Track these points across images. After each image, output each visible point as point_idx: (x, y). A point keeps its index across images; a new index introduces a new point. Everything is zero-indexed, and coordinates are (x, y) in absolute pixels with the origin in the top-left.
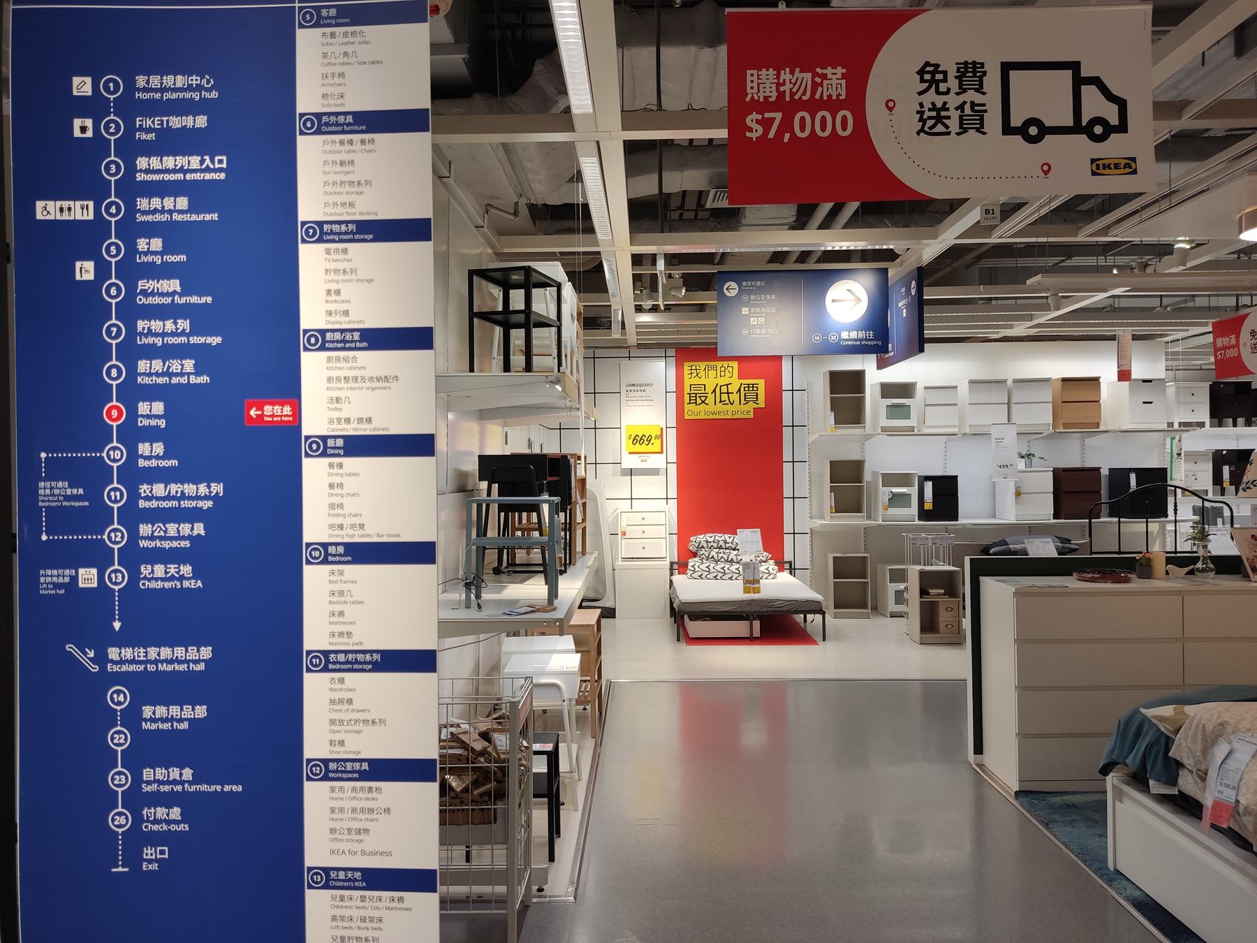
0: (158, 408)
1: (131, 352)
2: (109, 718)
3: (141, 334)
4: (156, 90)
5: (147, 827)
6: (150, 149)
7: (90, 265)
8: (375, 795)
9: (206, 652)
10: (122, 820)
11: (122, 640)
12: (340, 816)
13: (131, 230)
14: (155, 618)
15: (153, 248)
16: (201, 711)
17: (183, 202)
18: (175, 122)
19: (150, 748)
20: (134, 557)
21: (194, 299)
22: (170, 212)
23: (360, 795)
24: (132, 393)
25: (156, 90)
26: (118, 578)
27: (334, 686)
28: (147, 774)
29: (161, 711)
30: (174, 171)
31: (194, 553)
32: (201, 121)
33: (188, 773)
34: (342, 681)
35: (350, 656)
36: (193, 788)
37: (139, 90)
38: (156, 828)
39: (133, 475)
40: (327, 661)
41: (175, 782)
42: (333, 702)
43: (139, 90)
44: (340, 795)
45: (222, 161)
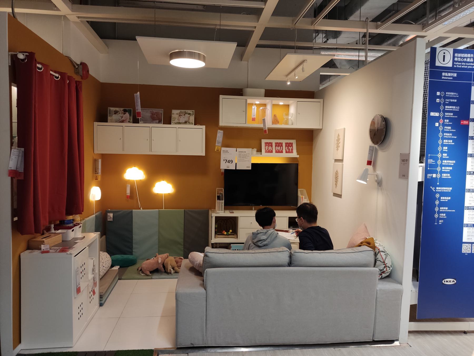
2: (436, 199)
5: (440, 217)
7: (438, 124)
11: (439, 186)
14: (444, 183)
19: (442, 204)
20: (441, 172)
26: (439, 176)
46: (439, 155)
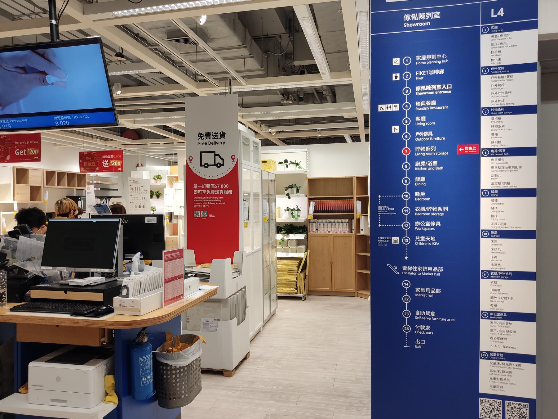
0: (423, 179)
1: (413, 159)
2: (403, 291)
3: (417, 152)
4: (424, 61)
6: (421, 83)
7: (397, 127)
8: (509, 325)
9: (441, 269)
10: (408, 329)
11: (408, 263)
12: (495, 333)
13: (413, 113)
14: (420, 255)
15: (422, 120)
16: (438, 291)
17: (434, 102)
18: (431, 72)
19: (419, 303)
20: (413, 233)
21: (438, 139)
22: (429, 106)
23: (503, 325)
24: (413, 174)
25: (424, 61)
26: (407, 241)
27: (493, 284)
28: (417, 313)
29: (423, 290)
30: (431, 91)
31: (436, 232)
32: (442, 71)
33: (433, 314)
34: (496, 282)
35: (500, 273)
36: (435, 319)
37: (417, 61)
38: (420, 333)
39: (413, 203)
40: (490, 275)
41: (428, 316)
42: (492, 290)
43: (417, 61)
44: (495, 325)
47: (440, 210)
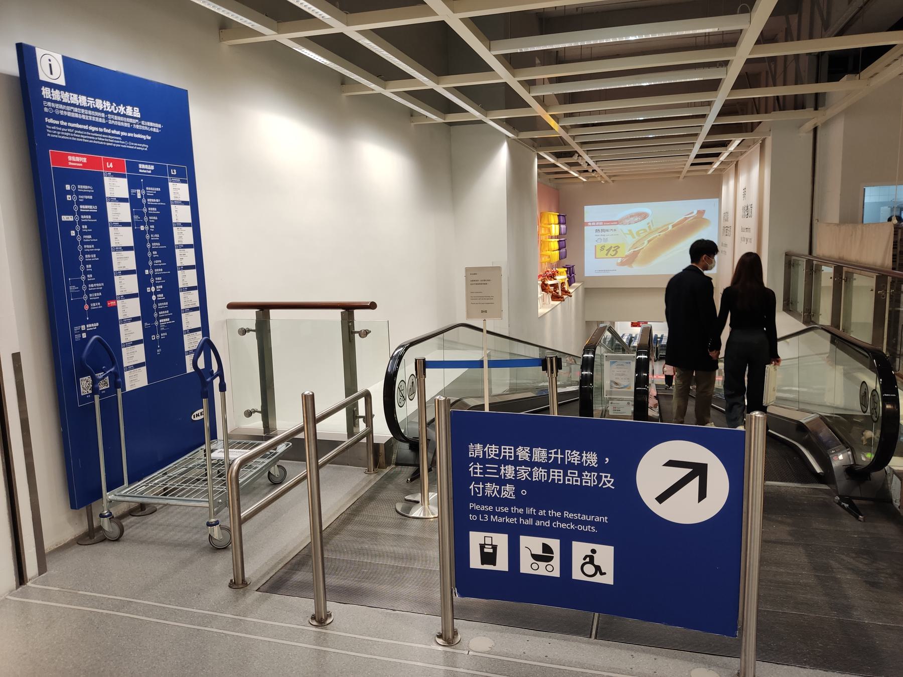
6: (83, 203)
45: (96, 207)
46: (83, 278)
47: (100, 285)
